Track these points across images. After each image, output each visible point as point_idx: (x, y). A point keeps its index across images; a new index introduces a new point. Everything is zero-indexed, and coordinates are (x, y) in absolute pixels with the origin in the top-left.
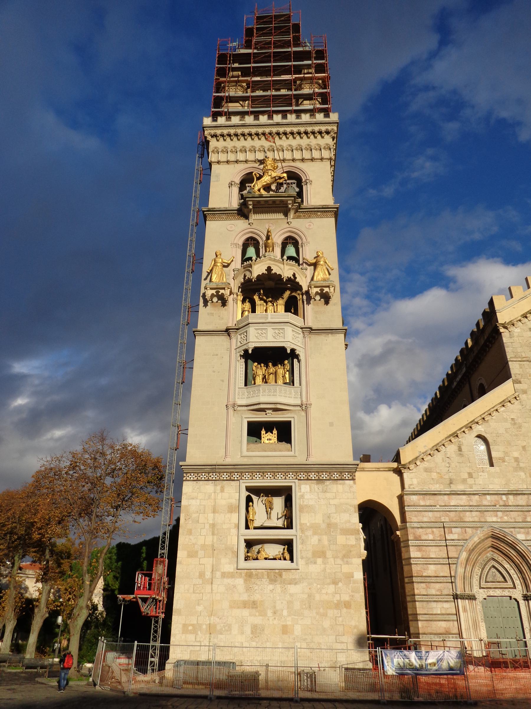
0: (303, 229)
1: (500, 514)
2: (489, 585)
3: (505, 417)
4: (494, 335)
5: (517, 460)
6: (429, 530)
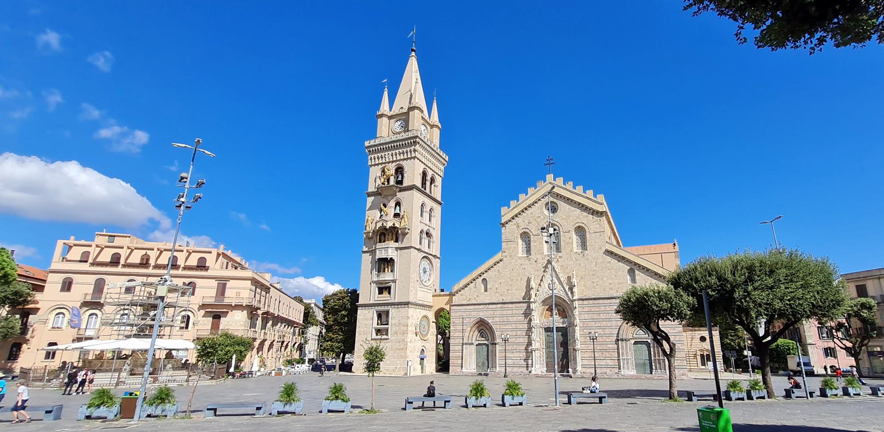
1: (485, 312)
2: (480, 339)
5: (497, 288)
6: (458, 319)
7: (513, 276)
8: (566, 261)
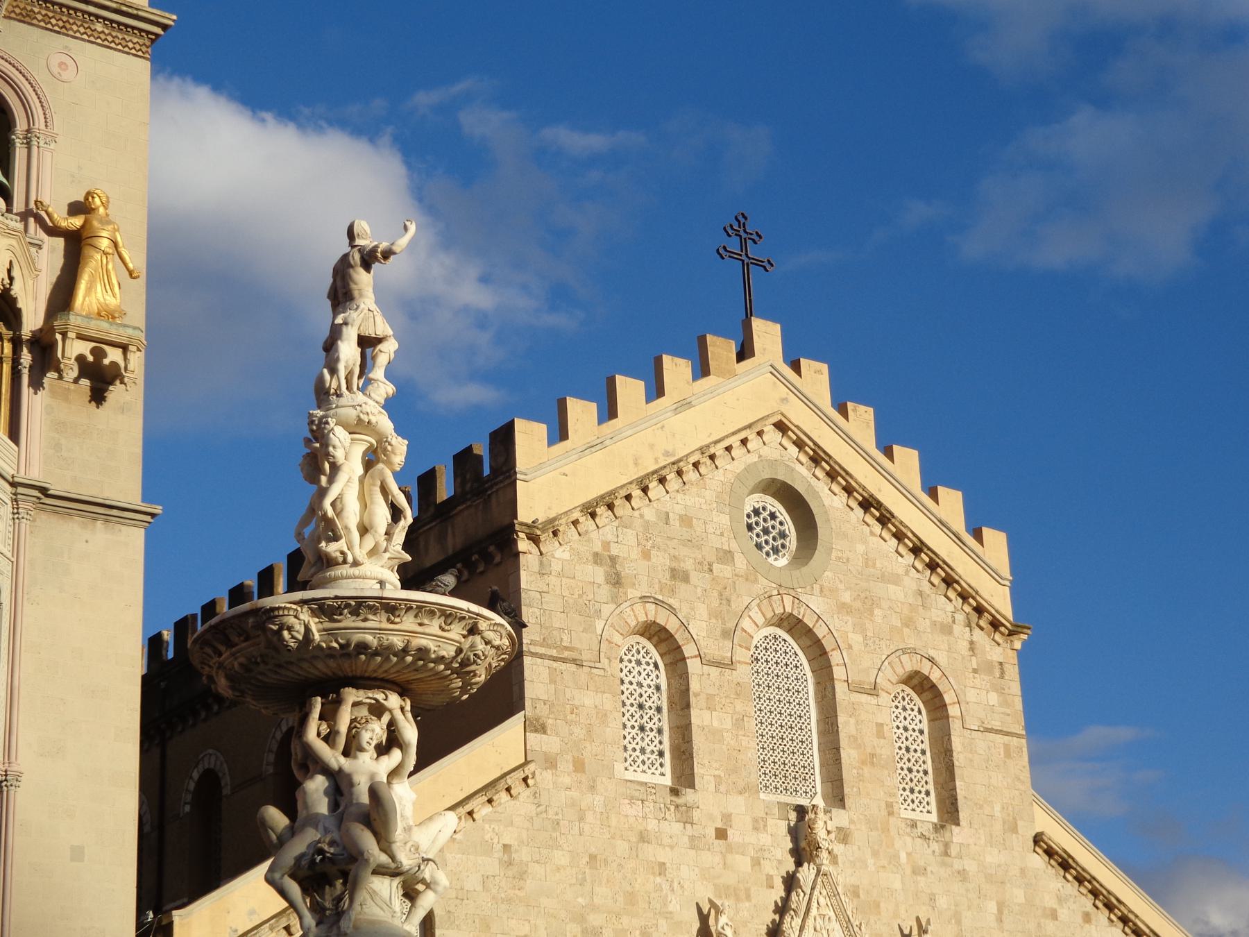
0: (40, 77)
3: (487, 837)
4: (492, 548)
7: (594, 908)
8: (870, 862)
